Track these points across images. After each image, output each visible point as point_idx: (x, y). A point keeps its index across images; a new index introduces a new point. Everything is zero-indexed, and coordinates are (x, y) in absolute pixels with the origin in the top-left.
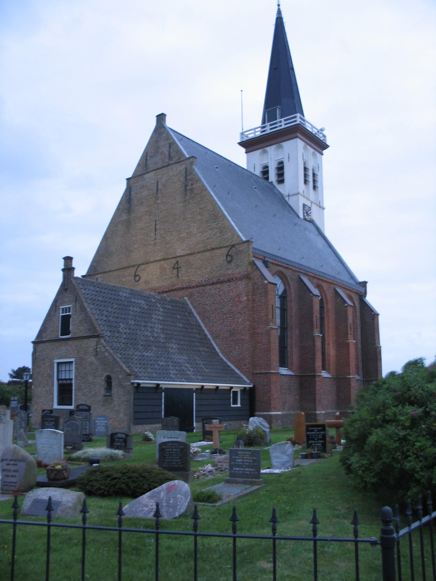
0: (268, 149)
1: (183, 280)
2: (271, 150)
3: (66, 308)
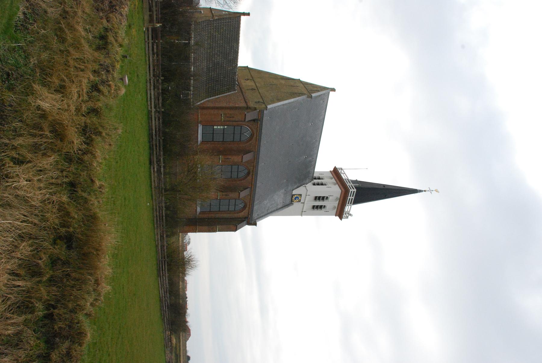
0: (334, 179)
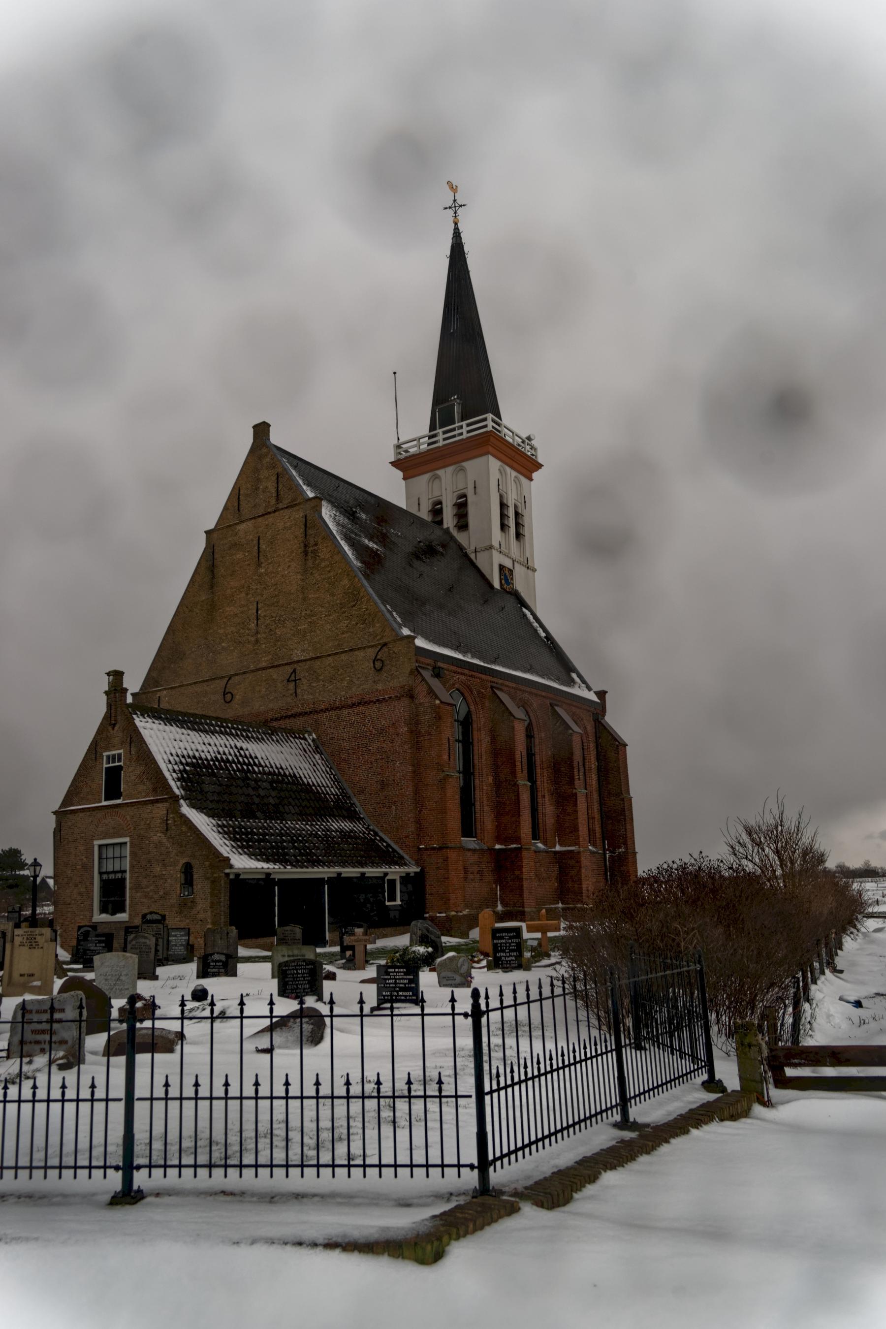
0: (440, 472)
1: (304, 699)
2: (446, 474)
3: (114, 756)
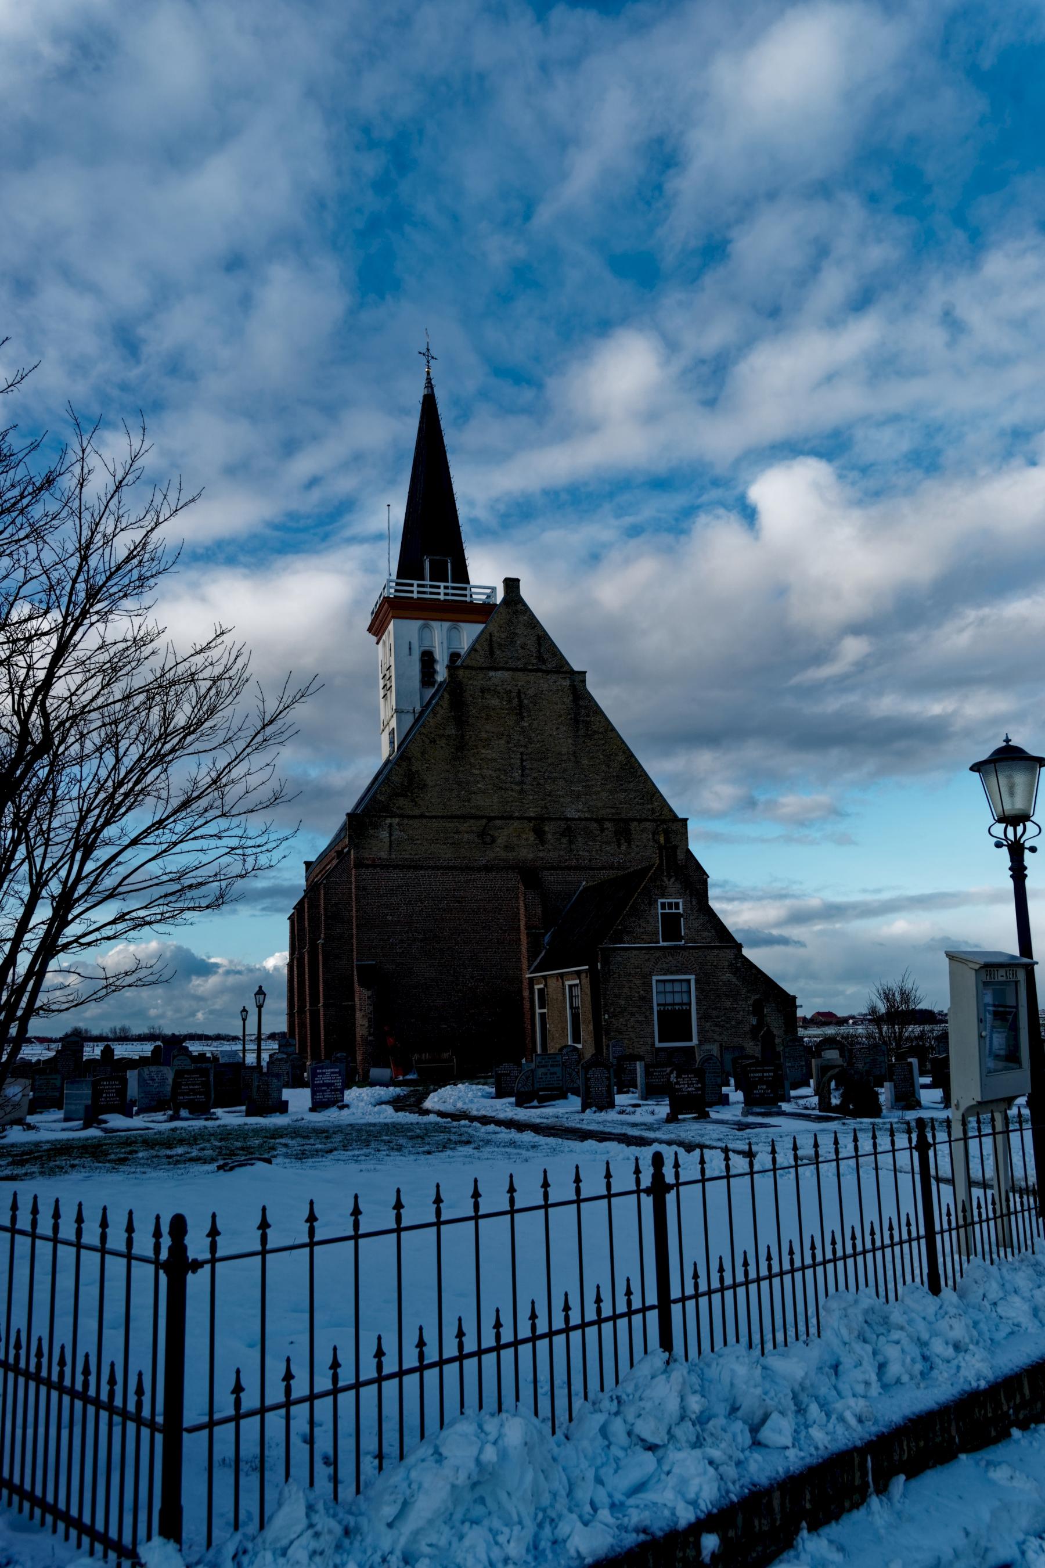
0: (434, 624)
